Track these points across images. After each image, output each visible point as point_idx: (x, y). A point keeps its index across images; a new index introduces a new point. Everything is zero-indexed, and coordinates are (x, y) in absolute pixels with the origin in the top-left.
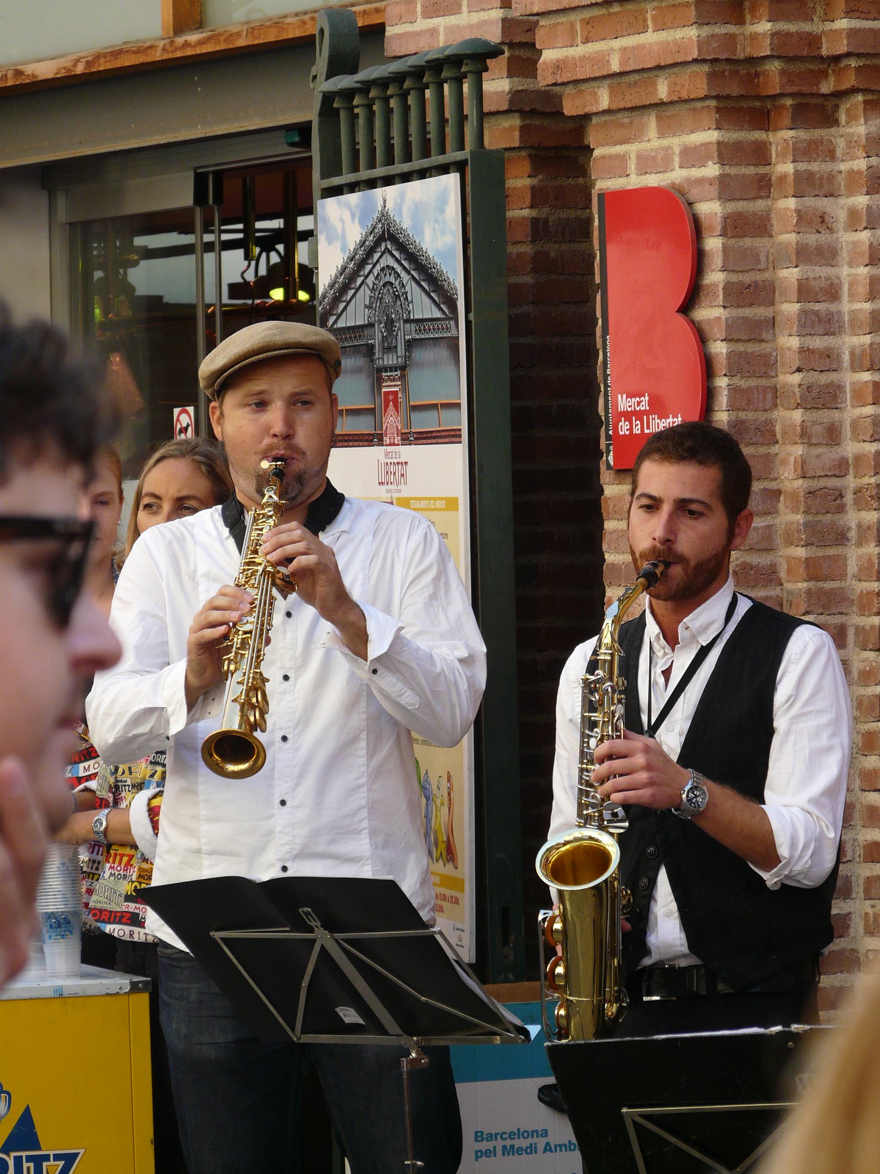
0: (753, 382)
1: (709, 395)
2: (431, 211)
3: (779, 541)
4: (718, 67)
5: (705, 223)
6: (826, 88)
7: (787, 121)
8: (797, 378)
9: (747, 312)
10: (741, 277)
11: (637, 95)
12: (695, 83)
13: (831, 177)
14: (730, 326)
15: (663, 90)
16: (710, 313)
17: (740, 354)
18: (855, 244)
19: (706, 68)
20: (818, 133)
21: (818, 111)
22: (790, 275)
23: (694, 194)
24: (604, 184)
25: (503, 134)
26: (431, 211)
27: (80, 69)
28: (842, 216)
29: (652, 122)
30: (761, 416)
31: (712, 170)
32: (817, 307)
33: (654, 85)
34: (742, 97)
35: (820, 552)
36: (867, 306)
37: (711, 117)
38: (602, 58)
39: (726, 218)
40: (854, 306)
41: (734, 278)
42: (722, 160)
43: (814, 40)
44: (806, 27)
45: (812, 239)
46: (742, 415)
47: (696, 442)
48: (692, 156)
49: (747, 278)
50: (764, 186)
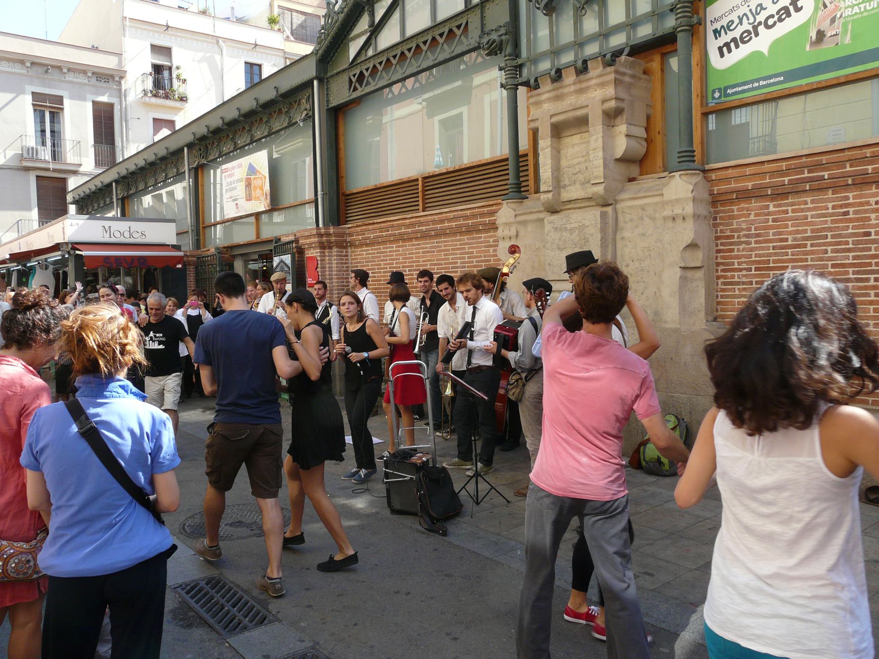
2: (287, 259)
11: (310, 246)
12: (317, 245)
21: (331, 248)
25: (295, 250)
26: (287, 259)
34: (322, 246)
47: (318, 282)
50: (324, 256)
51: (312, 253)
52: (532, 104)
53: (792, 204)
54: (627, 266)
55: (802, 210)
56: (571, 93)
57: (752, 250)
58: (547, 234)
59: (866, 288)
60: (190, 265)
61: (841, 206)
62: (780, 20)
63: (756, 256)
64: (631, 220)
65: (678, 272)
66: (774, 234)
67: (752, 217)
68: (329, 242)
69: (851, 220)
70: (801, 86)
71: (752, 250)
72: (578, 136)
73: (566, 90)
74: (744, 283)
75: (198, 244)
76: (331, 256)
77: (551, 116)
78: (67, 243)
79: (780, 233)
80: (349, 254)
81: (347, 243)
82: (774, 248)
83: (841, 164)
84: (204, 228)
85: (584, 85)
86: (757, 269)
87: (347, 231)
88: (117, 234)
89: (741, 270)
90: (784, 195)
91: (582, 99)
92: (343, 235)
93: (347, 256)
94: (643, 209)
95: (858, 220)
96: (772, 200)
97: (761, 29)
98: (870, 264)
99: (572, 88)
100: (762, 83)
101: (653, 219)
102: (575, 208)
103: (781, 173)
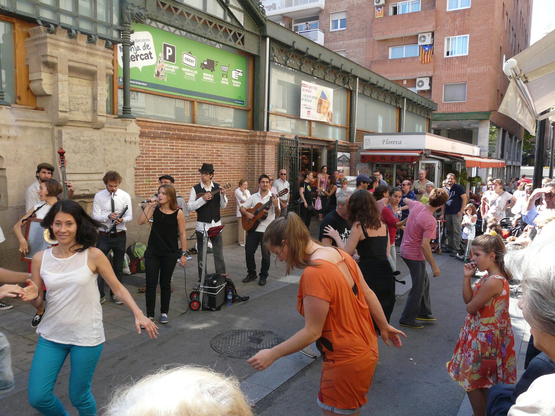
52: (51, 44)
53: (158, 142)
54: (107, 165)
55: (161, 145)
56: (83, 52)
57: (144, 160)
58: (65, 142)
59: (178, 177)
61: (172, 146)
62: (146, 59)
63: (146, 163)
64: (107, 140)
65: (134, 171)
66: (152, 154)
67: (144, 145)
69: (175, 152)
70: (159, 93)
71: (144, 160)
72: (78, 79)
73: (81, 48)
74: (141, 175)
77: (69, 60)
79: (154, 154)
82: (152, 160)
83: (174, 130)
85: (93, 51)
86: (146, 169)
89: (140, 169)
90: (154, 138)
91: (91, 60)
94: (115, 135)
95: (176, 152)
96: (151, 139)
97: (139, 58)
98: (179, 169)
99: (85, 50)
100: (139, 83)
101: (119, 141)
102: (74, 126)
103: (158, 128)
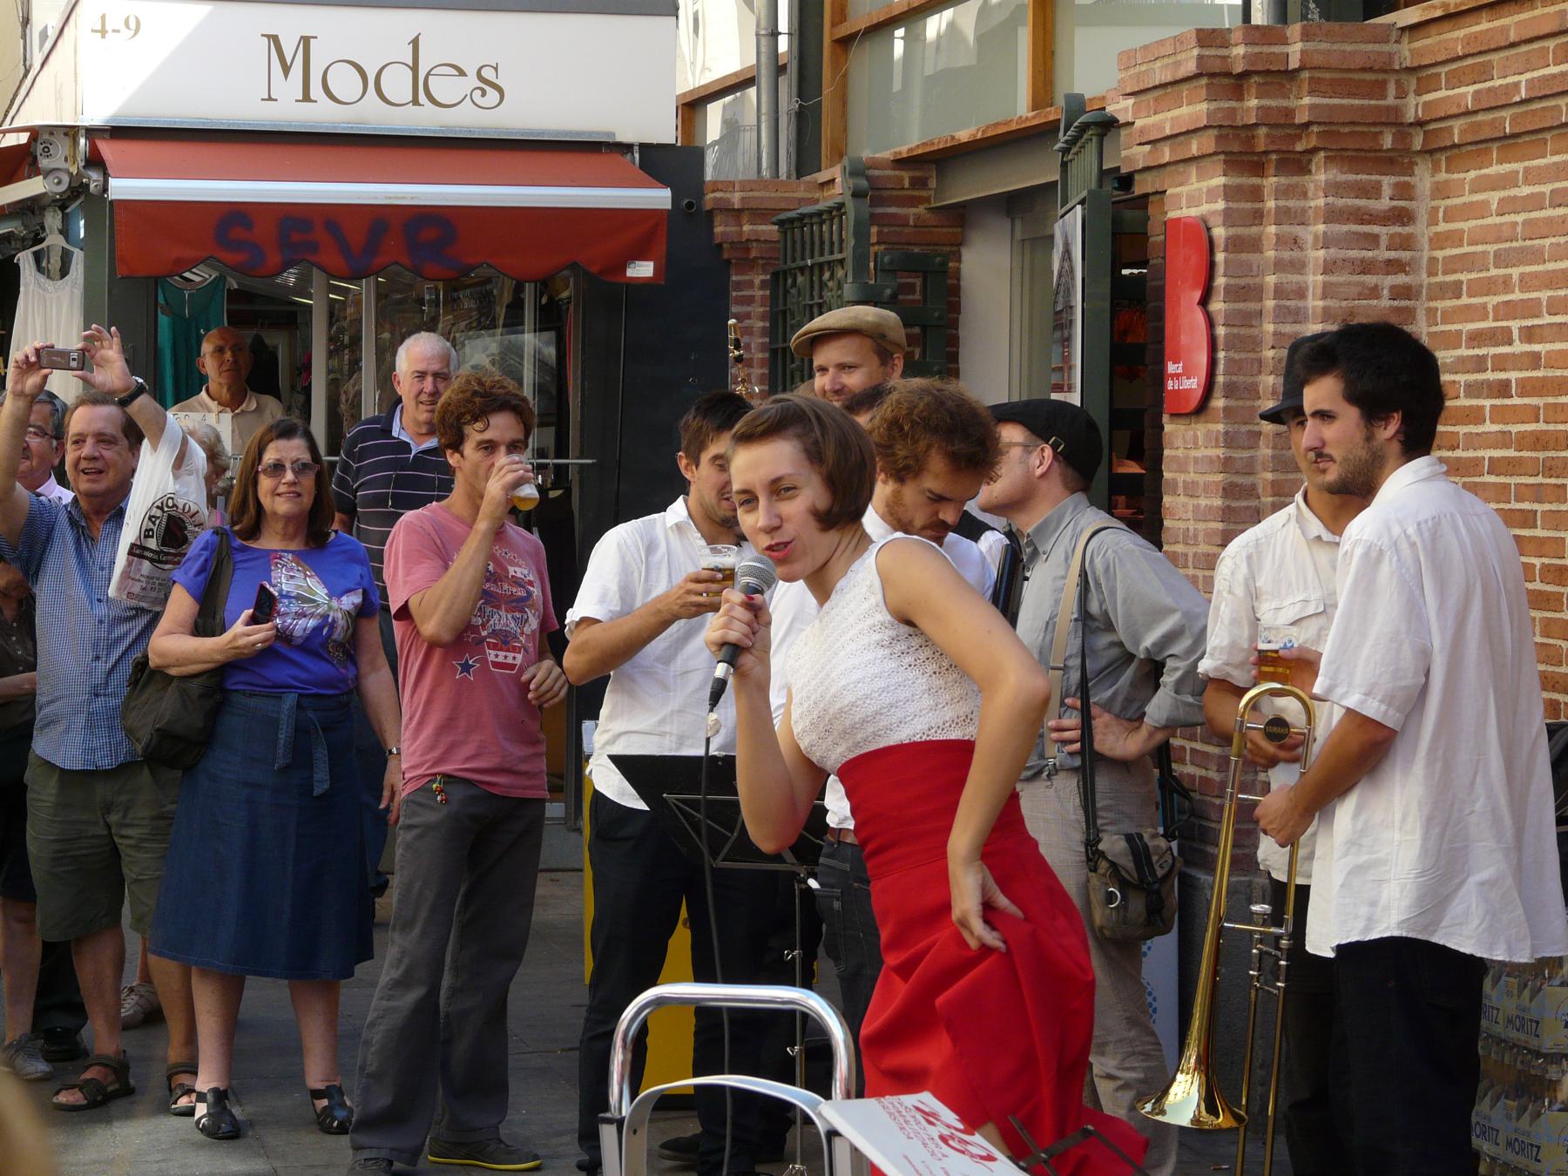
0: (1243, 355)
1: (1212, 363)
3: (1259, 468)
4: (1224, 132)
5: (1216, 242)
6: (1299, 147)
7: (1272, 171)
8: (1270, 353)
9: (1241, 306)
10: (1238, 281)
13: (1304, 211)
14: (1228, 315)
15: (1194, 148)
16: (1217, 306)
17: (1234, 336)
18: (1316, 259)
19: (1215, 132)
20: (1295, 179)
21: (1297, 164)
22: (1271, 280)
23: (1210, 224)
24: (1172, 215)
27: (979, 136)
28: (1310, 239)
29: (1193, 170)
30: (1249, 380)
31: (1220, 205)
32: (1288, 303)
33: (1189, 144)
34: (1243, 153)
35: (1282, 477)
36: (1321, 303)
37: (1220, 168)
38: (1160, 126)
39: (1228, 239)
40: (1314, 303)
41: (1232, 281)
42: (1227, 198)
43: (1289, 113)
44: (1284, 103)
45: (1286, 255)
46: (1234, 378)
48: (1211, 195)
49: (1242, 282)
50: (1258, 217)
51: (1196, 197)
60: (748, 264)
68: (1283, 124)
75: (808, 140)
76: (1300, 218)
78: (71, 132)
80: (1421, 208)
81: (1402, 128)
84: (845, 43)
87: (1406, 52)
88: (345, 83)
92: (1375, 76)
93: (1402, 217)
